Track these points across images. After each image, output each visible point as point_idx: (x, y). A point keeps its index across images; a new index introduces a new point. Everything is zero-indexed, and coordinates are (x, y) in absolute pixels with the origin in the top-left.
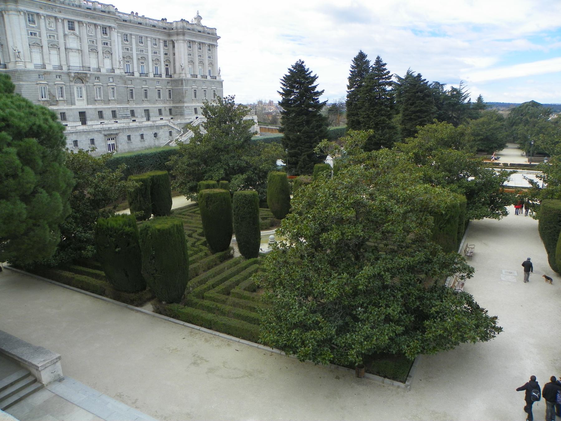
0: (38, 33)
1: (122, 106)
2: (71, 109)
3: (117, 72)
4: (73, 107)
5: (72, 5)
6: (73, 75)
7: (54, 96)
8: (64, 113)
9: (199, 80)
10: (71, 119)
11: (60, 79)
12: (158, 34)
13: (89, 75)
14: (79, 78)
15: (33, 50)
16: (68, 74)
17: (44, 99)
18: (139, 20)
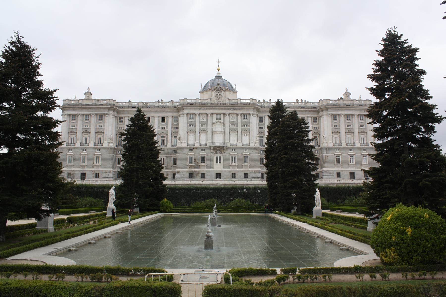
0: (194, 125)
1: (254, 170)
2: (210, 171)
3: (252, 145)
4: (211, 169)
5: (219, 104)
6: (212, 148)
7: (198, 163)
8: (204, 174)
9: (344, 147)
10: (208, 177)
11: (204, 151)
12: (307, 113)
13: (225, 148)
14: (218, 150)
15: (189, 135)
16: (210, 147)
17: (191, 164)
18: (303, 105)
